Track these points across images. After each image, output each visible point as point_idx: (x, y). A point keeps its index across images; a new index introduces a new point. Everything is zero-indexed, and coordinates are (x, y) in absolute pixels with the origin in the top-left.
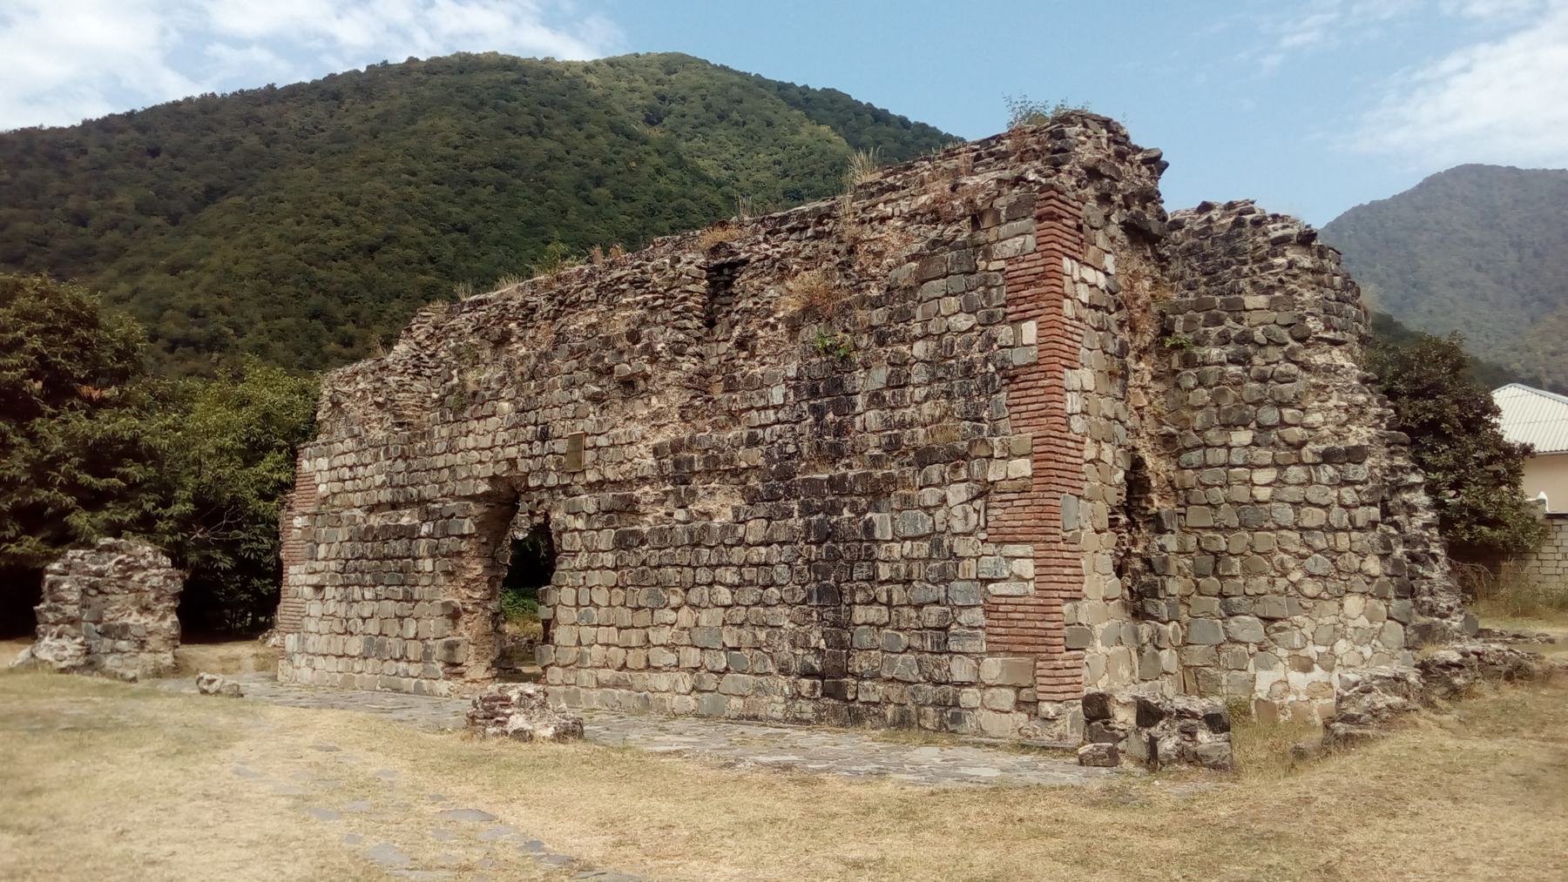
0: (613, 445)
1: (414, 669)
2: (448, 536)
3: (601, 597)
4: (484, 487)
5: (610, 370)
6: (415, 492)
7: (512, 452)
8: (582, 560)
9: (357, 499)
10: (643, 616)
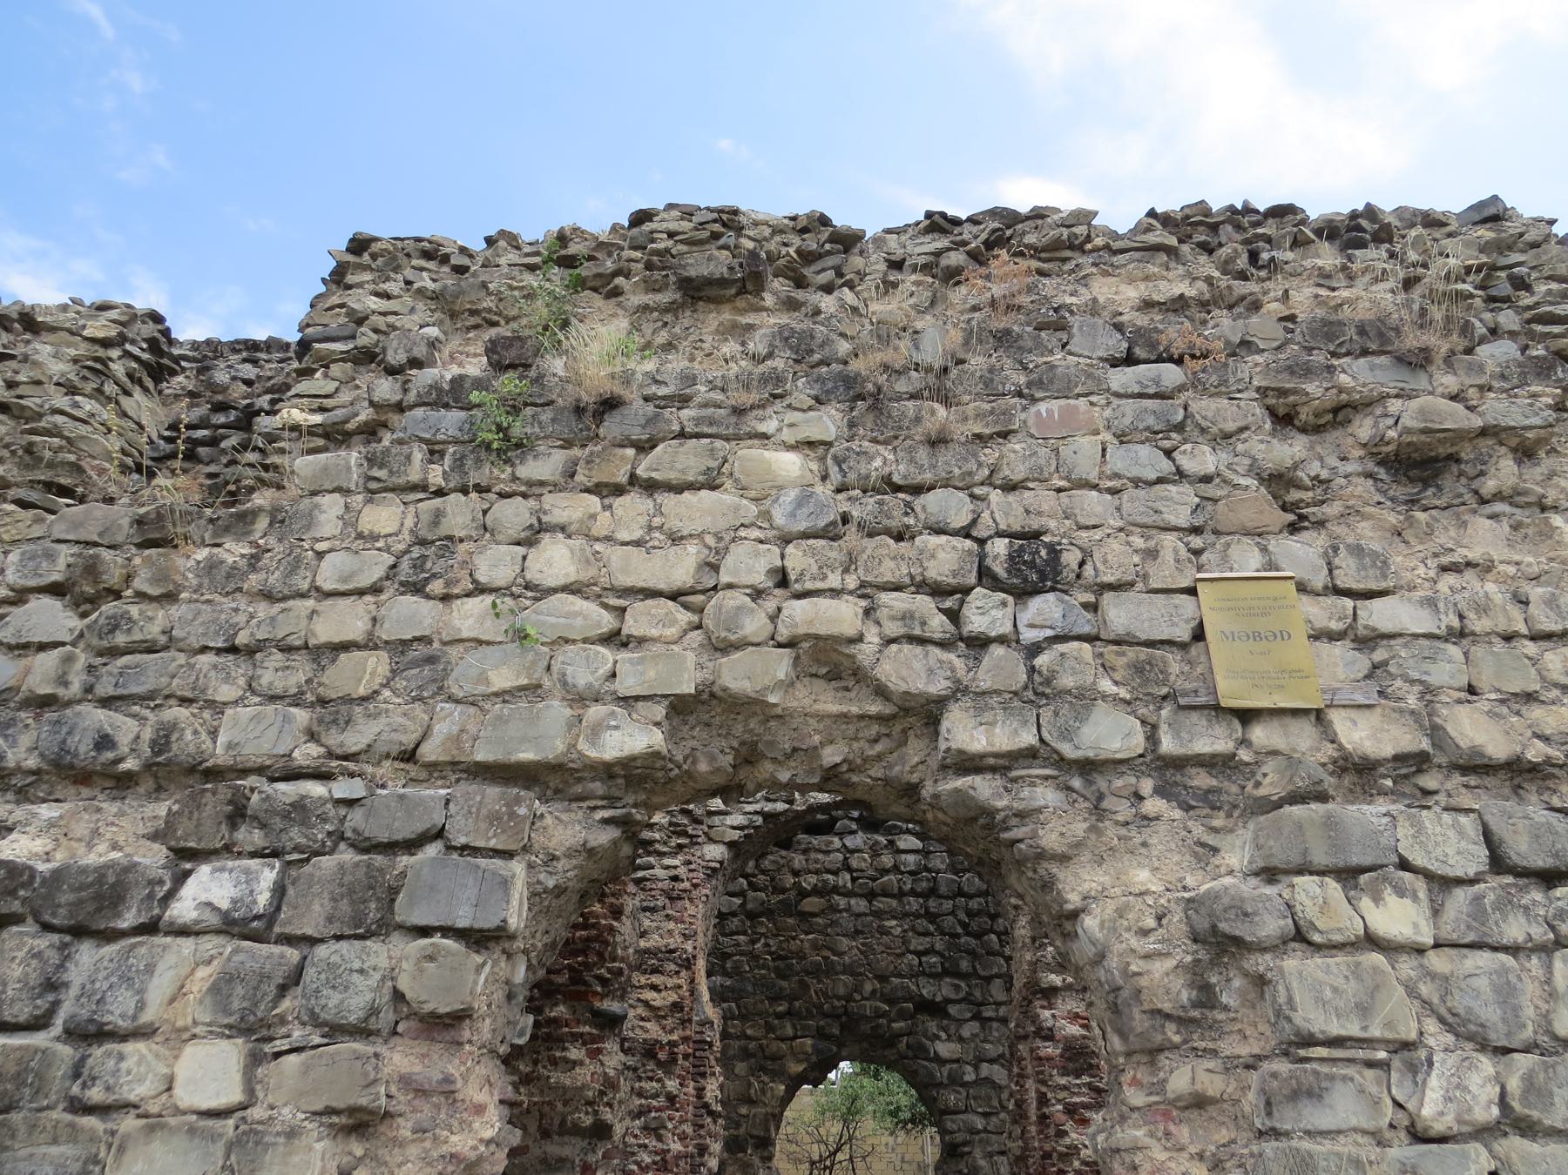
0: (1459, 634)
2: (384, 928)
4: (629, 738)
5: (1341, 413)
6: (127, 729)
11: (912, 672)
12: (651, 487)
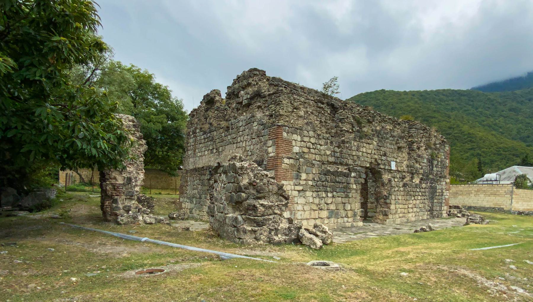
1: (350, 220)
3: (400, 198)
7: (376, 157)
8: (396, 189)
9: (318, 158)
10: (408, 202)
11: (379, 162)
12: (368, 144)
